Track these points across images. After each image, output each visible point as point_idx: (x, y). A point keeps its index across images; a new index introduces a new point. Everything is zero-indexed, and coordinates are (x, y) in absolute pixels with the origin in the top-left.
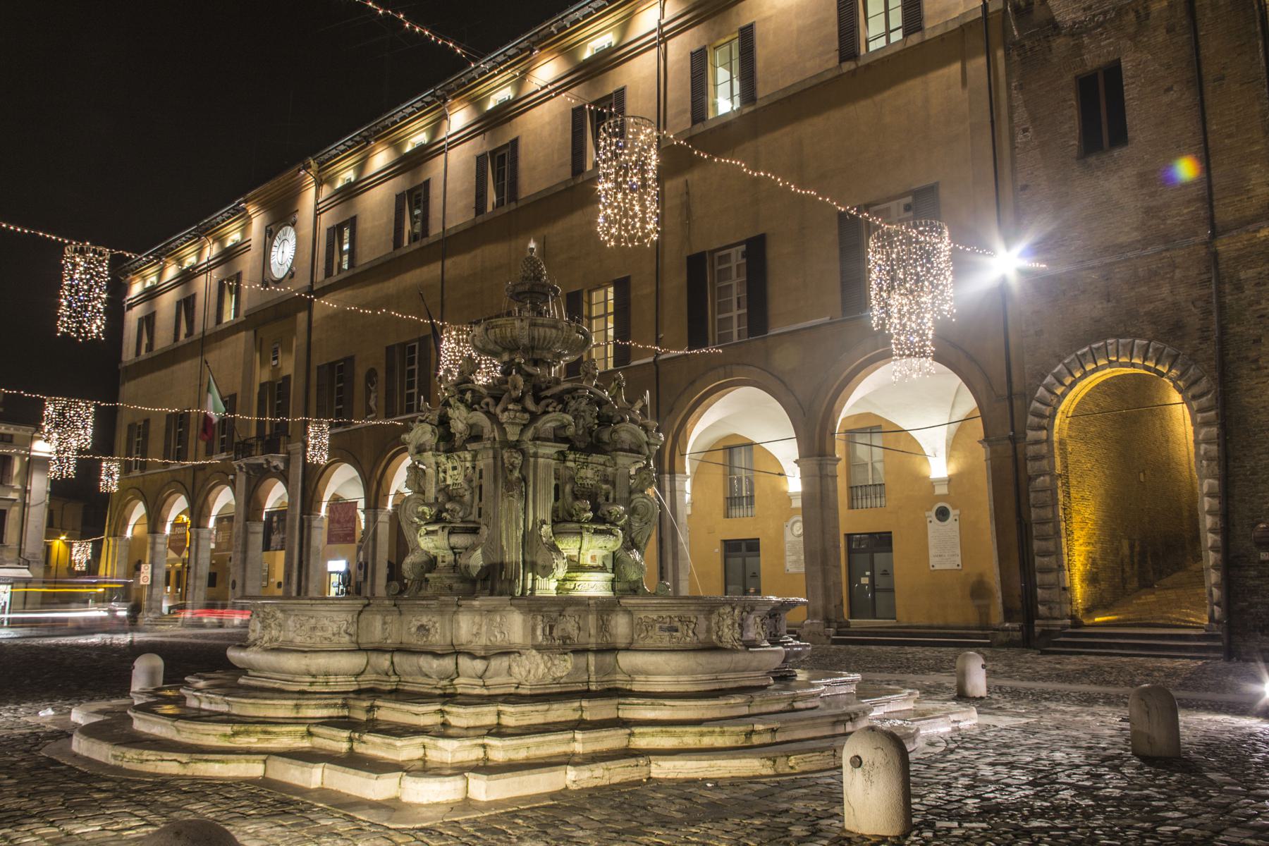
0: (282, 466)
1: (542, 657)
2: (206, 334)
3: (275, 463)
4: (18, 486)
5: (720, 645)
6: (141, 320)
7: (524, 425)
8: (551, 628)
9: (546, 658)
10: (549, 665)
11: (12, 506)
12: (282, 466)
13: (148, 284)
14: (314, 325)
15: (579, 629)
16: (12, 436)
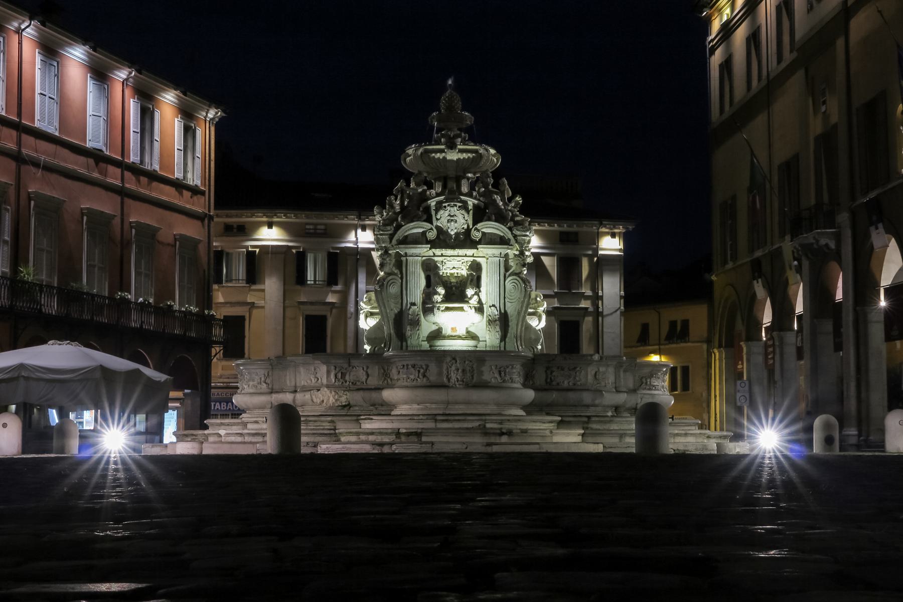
0: (832, 245)
1: (331, 392)
2: (771, 78)
3: (823, 242)
4: (589, 293)
5: (447, 384)
6: (721, 66)
7: (391, 234)
8: (343, 375)
9: (333, 393)
10: (336, 397)
11: (584, 316)
12: (832, 245)
13: (725, 18)
14: (852, 53)
15: (368, 375)
16: (576, 234)
